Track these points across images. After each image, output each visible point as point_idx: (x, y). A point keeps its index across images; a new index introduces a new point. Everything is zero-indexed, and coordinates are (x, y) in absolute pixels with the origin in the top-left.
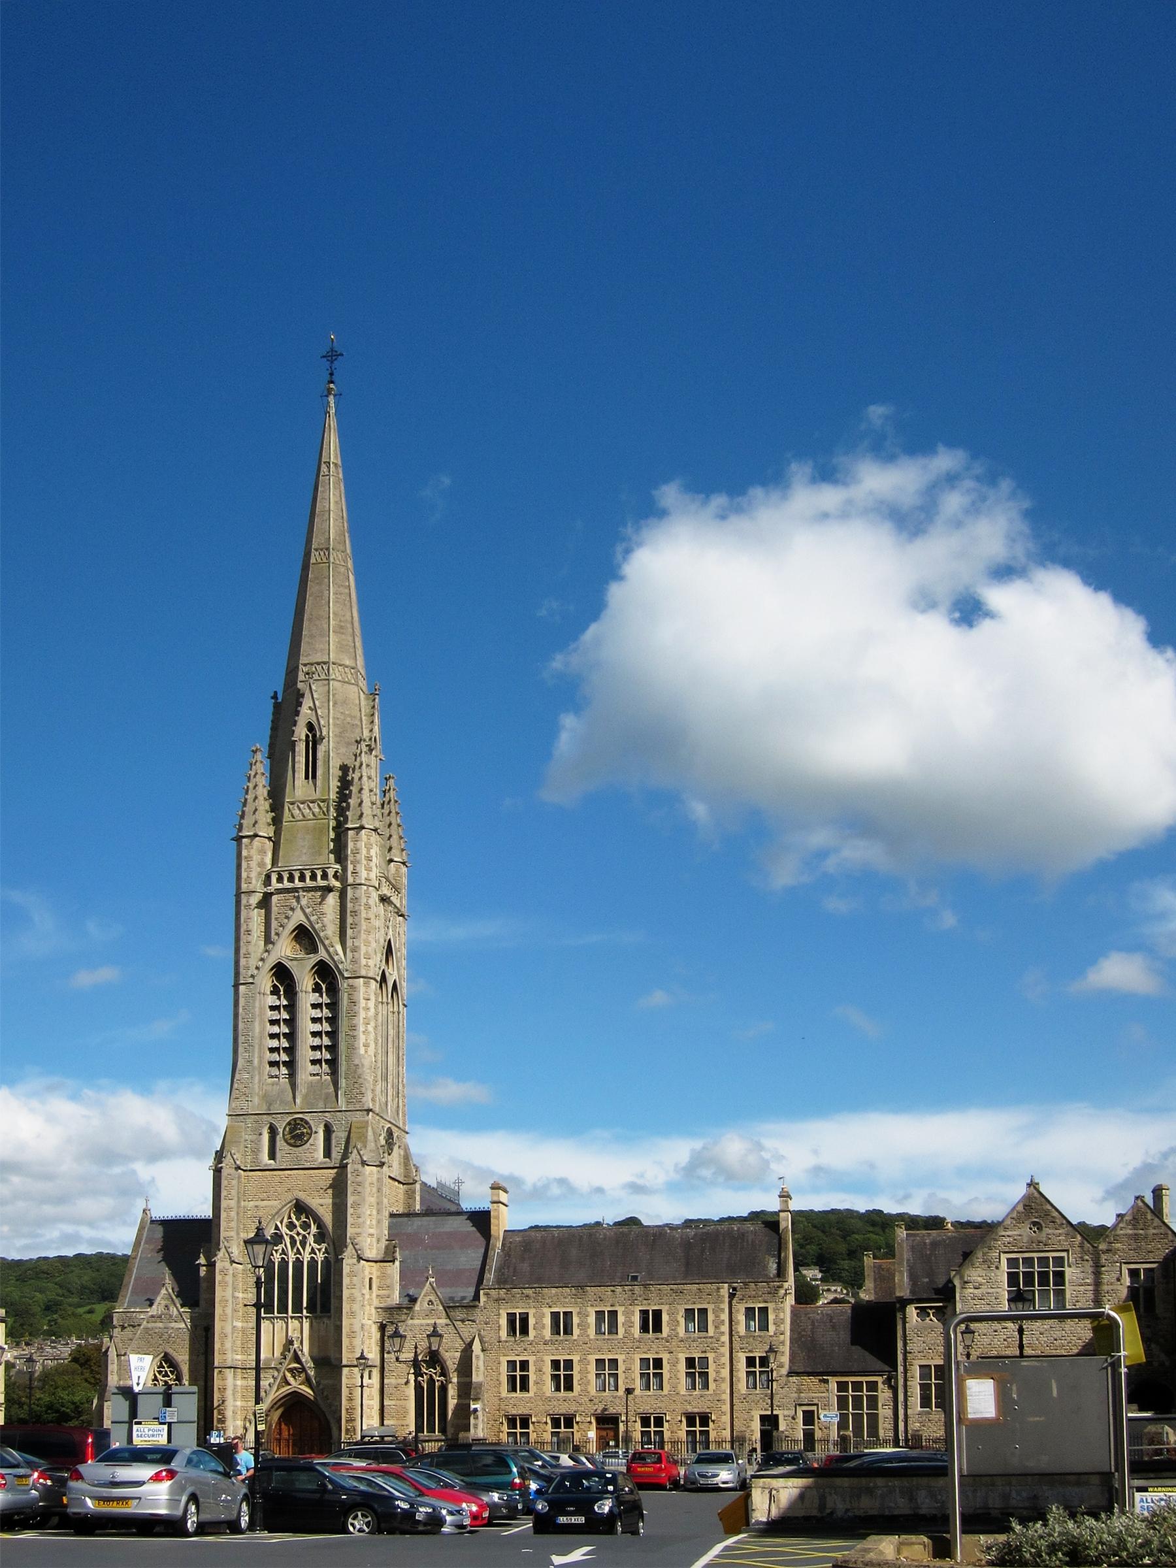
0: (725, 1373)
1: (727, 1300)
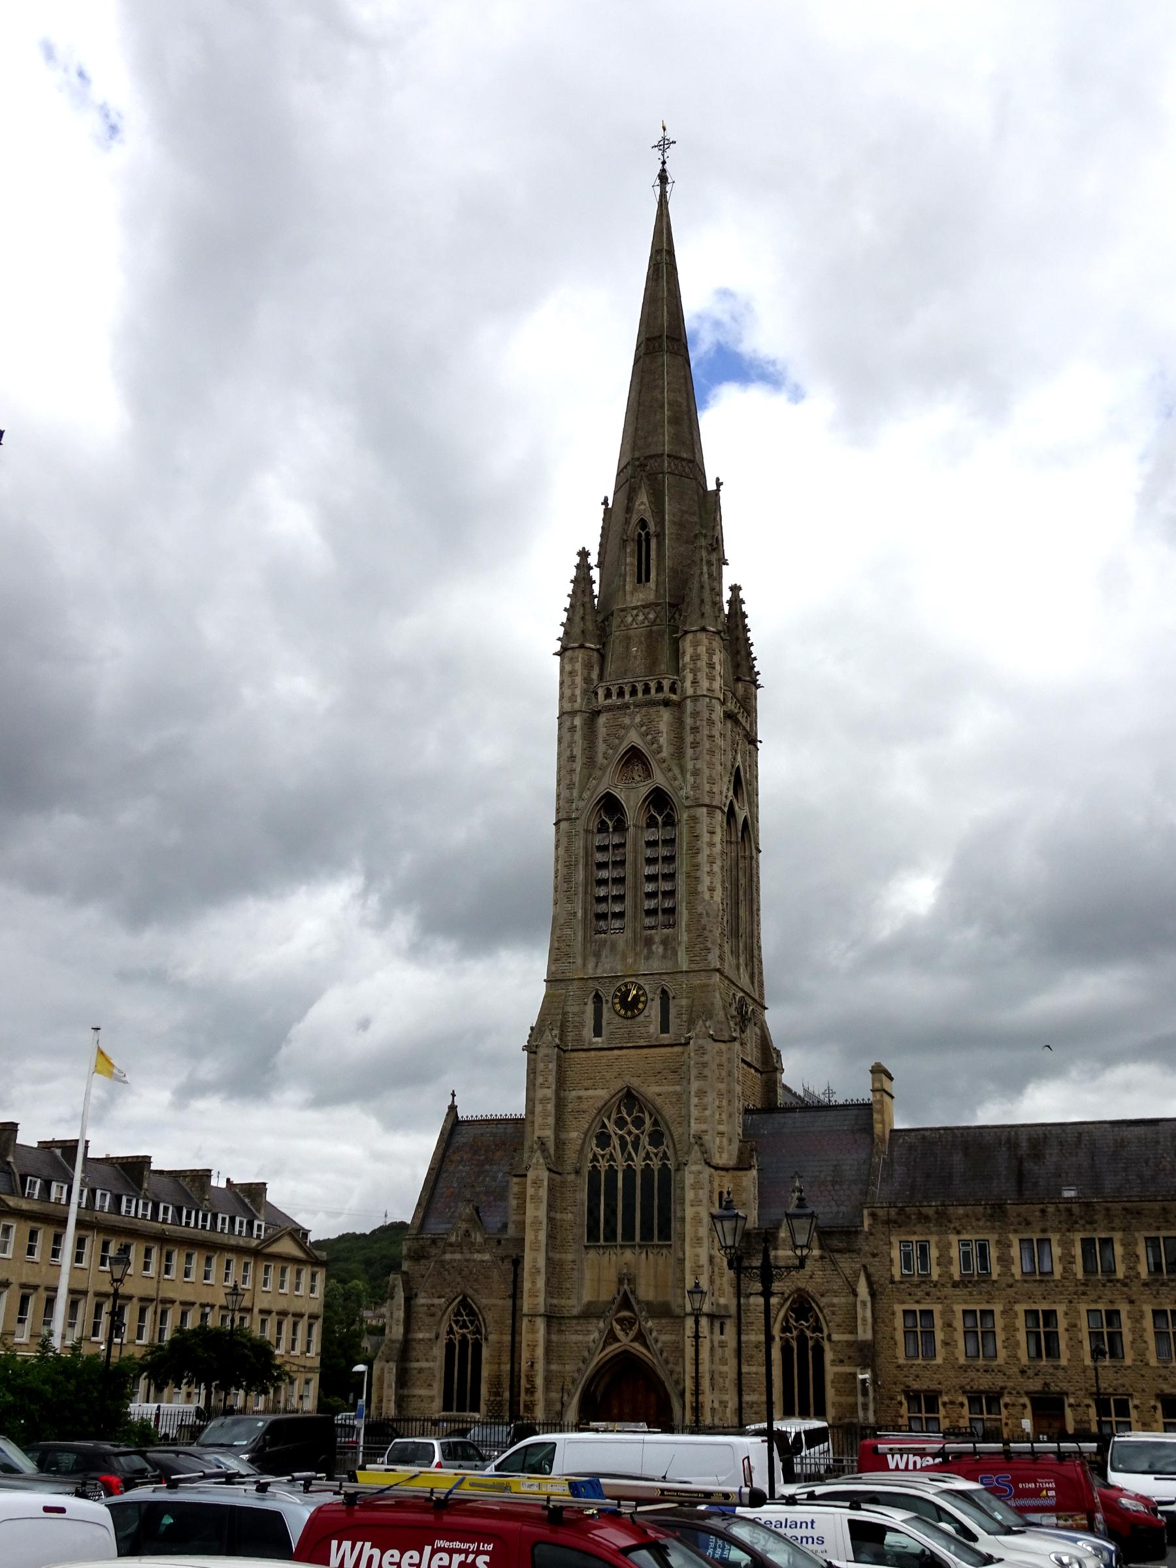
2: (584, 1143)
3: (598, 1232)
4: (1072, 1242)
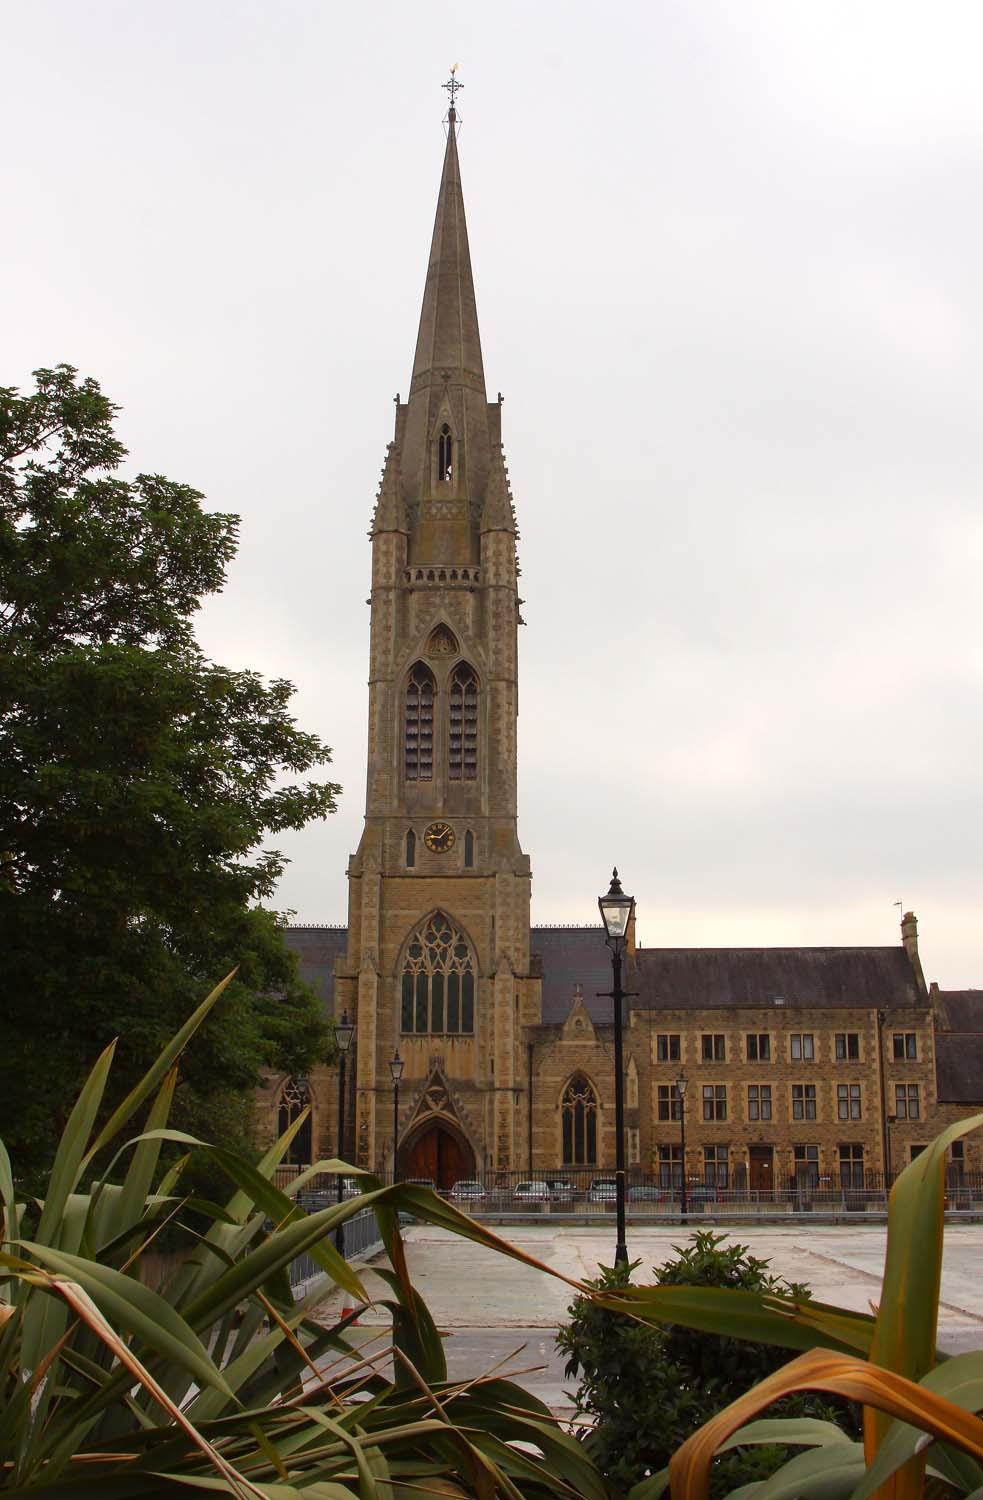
0: (877, 1101)
1: (876, 1025)
2: (399, 955)
3: (413, 1023)
4: (829, 1036)
